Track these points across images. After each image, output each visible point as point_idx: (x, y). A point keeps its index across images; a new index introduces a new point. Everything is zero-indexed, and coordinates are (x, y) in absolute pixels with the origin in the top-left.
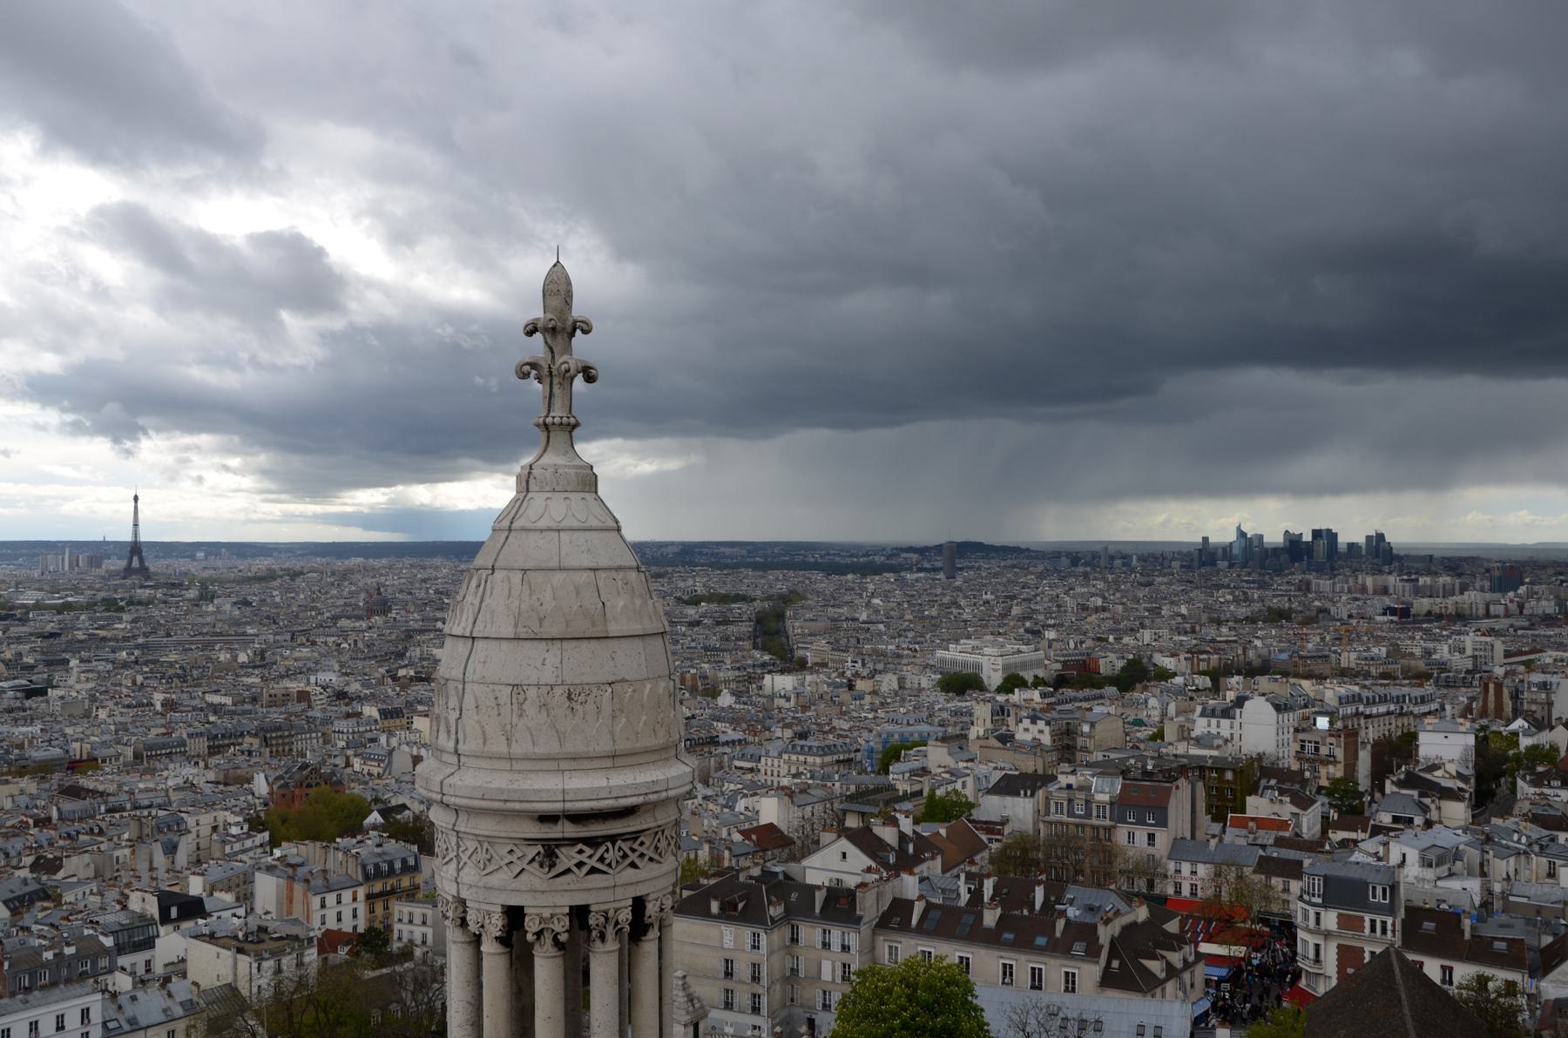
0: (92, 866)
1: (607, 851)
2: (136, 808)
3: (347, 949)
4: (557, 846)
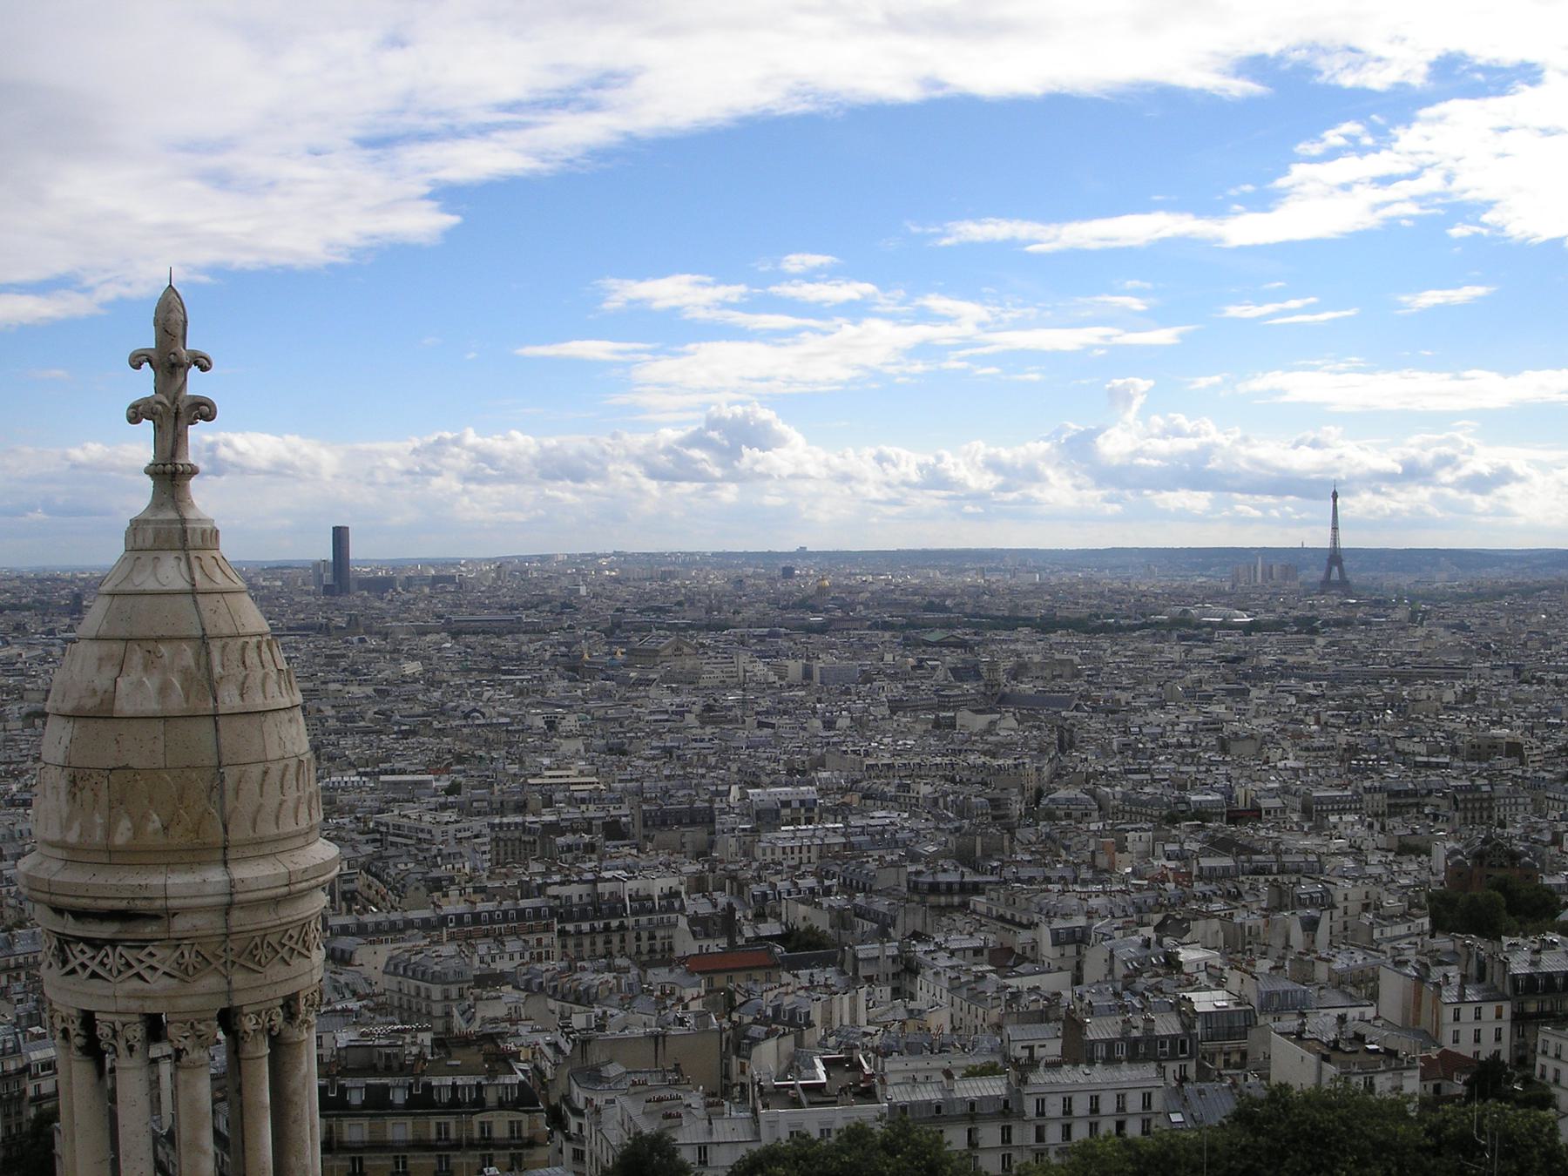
0: (1221, 935)
1: (107, 955)
2: (1282, 871)
3: (1465, 1077)
4: (67, 942)
